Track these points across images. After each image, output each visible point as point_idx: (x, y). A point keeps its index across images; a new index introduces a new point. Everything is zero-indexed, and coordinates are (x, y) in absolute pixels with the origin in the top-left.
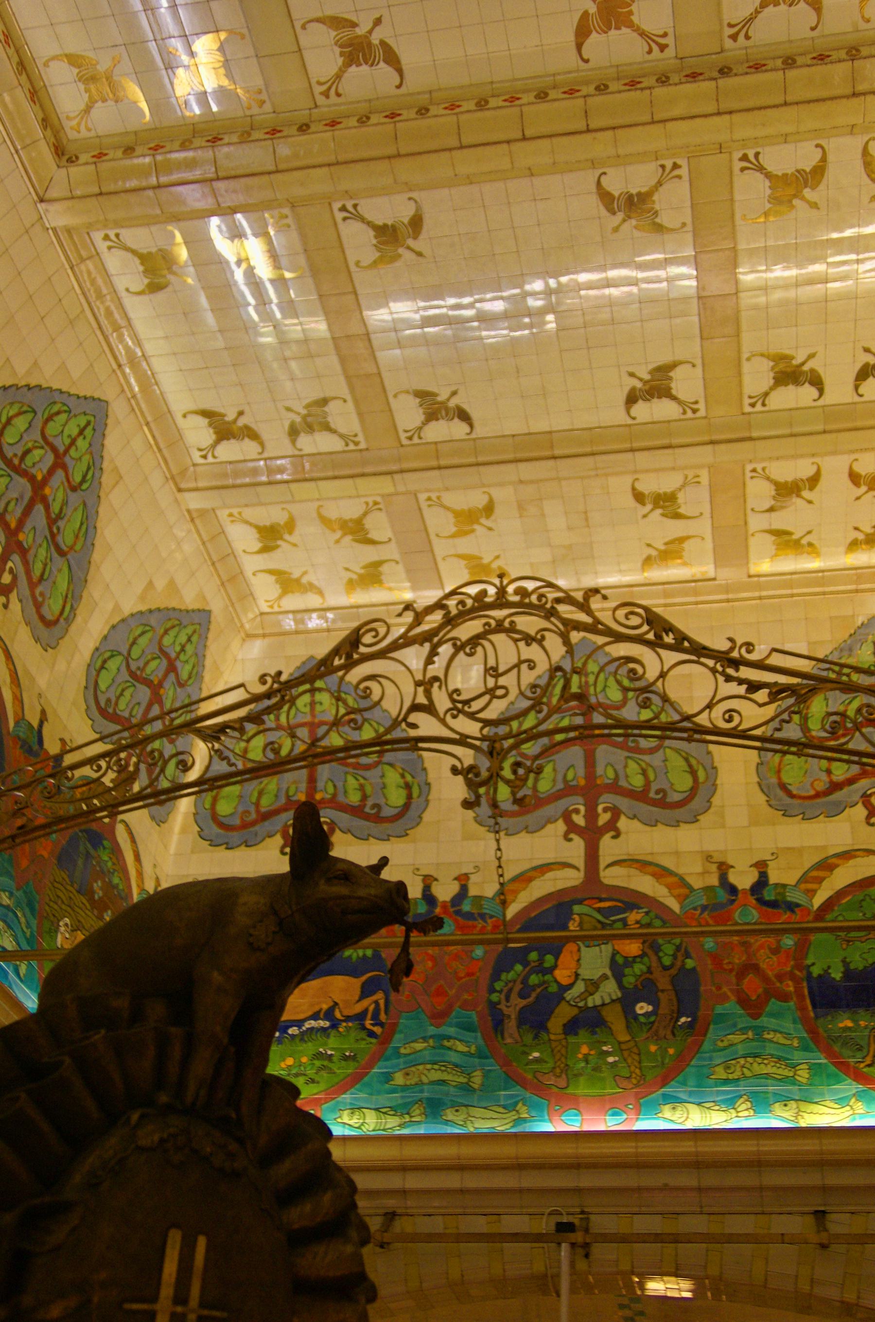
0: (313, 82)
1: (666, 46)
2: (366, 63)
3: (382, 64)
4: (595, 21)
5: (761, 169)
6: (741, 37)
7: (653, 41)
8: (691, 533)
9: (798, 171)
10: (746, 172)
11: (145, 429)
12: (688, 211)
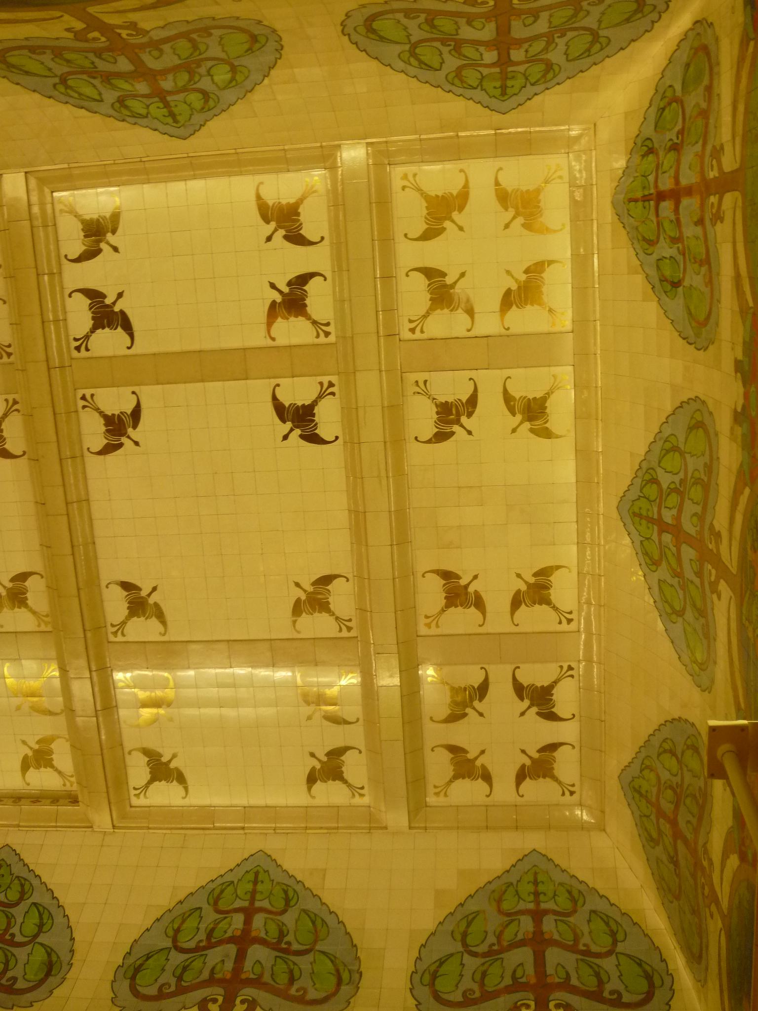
0: (37, 629)
1: (14, 400)
2: (25, 594)
3: (27, 584)
5: (87, 337)
7: (11, 408)
8: (501, 390)
9: (90, 309)
11: (308, 831)
12: (122, 389)
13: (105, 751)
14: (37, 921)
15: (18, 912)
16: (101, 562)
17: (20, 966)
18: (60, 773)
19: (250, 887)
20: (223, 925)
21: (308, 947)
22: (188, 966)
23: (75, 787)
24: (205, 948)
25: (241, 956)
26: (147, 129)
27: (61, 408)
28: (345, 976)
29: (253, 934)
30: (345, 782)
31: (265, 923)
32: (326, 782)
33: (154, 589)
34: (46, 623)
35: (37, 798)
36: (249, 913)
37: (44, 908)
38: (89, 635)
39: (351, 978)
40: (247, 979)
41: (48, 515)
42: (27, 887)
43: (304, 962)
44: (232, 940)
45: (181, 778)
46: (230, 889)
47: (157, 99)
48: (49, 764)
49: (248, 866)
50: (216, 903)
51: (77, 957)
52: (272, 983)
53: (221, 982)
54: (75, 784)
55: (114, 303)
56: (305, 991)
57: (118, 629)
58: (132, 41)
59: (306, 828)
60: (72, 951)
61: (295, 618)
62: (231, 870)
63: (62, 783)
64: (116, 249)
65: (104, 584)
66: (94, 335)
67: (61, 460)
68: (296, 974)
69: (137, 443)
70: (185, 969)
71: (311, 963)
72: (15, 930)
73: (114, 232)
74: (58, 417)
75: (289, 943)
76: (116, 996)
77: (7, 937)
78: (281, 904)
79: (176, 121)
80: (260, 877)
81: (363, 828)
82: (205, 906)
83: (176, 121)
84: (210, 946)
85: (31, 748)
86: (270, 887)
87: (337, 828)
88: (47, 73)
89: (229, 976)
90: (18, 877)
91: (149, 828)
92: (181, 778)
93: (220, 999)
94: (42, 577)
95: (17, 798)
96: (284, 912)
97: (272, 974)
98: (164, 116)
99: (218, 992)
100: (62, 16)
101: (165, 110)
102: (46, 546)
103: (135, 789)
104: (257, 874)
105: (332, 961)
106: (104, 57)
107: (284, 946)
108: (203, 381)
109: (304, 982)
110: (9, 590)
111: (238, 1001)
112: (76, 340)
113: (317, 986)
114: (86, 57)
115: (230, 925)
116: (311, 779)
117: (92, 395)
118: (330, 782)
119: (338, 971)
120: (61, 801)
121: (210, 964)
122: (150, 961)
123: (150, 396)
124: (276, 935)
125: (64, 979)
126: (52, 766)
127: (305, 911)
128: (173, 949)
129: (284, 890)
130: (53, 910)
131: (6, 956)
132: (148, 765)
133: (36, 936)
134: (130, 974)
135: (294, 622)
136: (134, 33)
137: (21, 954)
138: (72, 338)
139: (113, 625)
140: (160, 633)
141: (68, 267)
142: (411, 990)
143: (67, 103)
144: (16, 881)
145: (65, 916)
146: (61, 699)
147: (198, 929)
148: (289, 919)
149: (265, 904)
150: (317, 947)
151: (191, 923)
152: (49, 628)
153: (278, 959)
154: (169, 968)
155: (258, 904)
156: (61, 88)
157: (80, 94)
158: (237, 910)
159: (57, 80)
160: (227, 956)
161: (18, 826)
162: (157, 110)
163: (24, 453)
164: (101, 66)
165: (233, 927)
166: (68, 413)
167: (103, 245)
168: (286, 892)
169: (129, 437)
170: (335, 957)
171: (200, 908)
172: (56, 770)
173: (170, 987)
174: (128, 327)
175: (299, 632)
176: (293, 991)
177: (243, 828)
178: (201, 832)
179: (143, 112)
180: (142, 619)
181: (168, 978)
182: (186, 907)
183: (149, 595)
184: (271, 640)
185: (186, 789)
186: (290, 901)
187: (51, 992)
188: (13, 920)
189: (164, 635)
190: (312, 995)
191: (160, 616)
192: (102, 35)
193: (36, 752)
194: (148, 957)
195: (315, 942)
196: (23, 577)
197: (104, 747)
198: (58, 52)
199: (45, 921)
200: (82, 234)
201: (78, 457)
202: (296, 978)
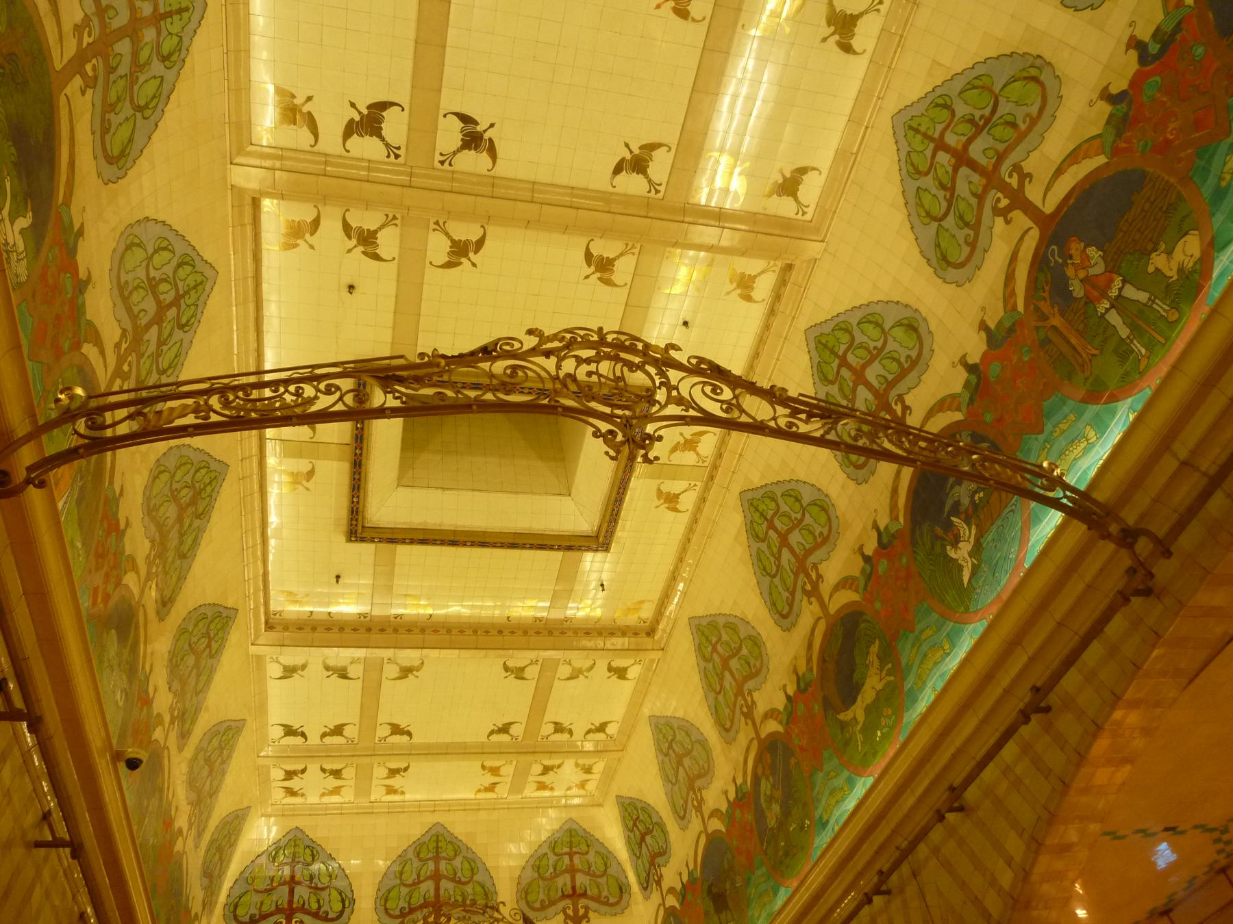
0: (636, 256)
1: (434, 223)
4: (472, 247)
5: (387, 145)
6: (391, 217)
9: (362, 136)
10: (397, 146)
11: (893, 67)
12: (440, 127)
13: (756, 230)
14: (871, 326)
15: (859, 338)
16: (592, 186)
17: (900, 350)
18: (762, 272)
19: (919, 137)
20: (940, 172)
21: (992, 102)
22: (960, 214)
23: (779, 263)
24: (952, 195)
25: (973, 165)
26: (194, 39)
27: (446, 185)
28: (1033, 72)
29: (959, 147)
30: (861, 15)
31: (955, 133)
32: (854, 35)
33: (627, 145)
34: (633, 247)
35: (777, 297)
36: (941, 145)
37: (864, 317)
38: (651, 214)
39: (1037, 67)
40: (994, 165)
41: (539, 221)
42: (843, 326)
43: (1004, 108)
44: (956, 169)
45: (803, 171)
46: (914, 156)
47: (162, 23)
48: (753, 279)
49: (901, 133)
50: (918, 172)
51: (912, 303)
52: (1007, 144)
53: (986, 190)
54: (777, 262)
55: (360, 113)
56: (1028, 115)
57: (655, 188)
58: (97, 33)
59: (890, 67)
60: (906, 306)
61: (690, 19)
62: (898, 150)
63: (771, 273)
64: (309, 99)
65: (611, 189)
66: (386, 139)
67: (492, 197)
68: (1009, 118)
69: (492, 125)
70: (961, 218)
71: (1008, 101)
72: (872, 345)
73: (293, 96)
74: (454, 189)
75: (982, 117)
76: (957, 282)
77: (875, 352)
78: (945, 114)
79: (187, 9)
80: (915, 126)
81: (912, 9)
82: (918, 183)
83: (187, 9)
84: (952, 190)
85: (735, 289)
86: (927, 119)
87: (901, 36)
88: (132, 121)
89: (984, 181)
90: (833, 330)
91: (835, 212)
92: (803, 171)
93: (999, 195)
94: (592, 240)
95: (772, 312)
96: (953, 113)
97: (1000, 142)
98: (181, 20)
99: (994, 194)
100: (66, 95)
101: (174, 17)
102: (566, 229)
103: (797, 214)
104: (911, 128)
105: (1015, 81)
106: (114, 65)
107: (981, 123)
108: (444, 47)
109: (1020, 113)
110: (597, 270)
111: (1007, 180)
112: (388, 156)
113: (1029, 102)
114: (114, 82)
115: (943, 166)
116: (847, 48)
117: (441, 154)
118: (856, 30)
119: (1025, 78)
120: (787, 278)
121: (967, 195)
122: (942, 246)
123: (451, 101)
124: (969, 126)
125: (925, 319)
126: (755, 277)
127: (961, 93)
128: (941, 223)
129: (934, 107)
130: (869, 310)
131: (888, 358)
132: (780, 196)
133: (883, 330)
134: (944, 265)
135: (694, 20)
136: (87, 29)
137: (891, 345)
138: (386, 160)
139: (649, 192)
140: (668, 151)
141: (320, 147)
142: (1076, 10)
143: (163, 111)
144: (836, 332)
145: (877, 303)
146: (702, 254)
147: (934, 195)
148: (961, 110)
149: (940, 128)
150: (997, 92)
151: (927, 199)
152: (638, 246)
153: (991, 132)
154: (955, 231)
155: (936, 135)
156: (148, 113)
157: (154, 97)
158: (934, 156)
159: (139, 115)
160: (967, 177)
161: (794, 318)
162: (174, 25)
163: (482, 226)
164: (124, 69)
165: (946, 164)
166: (453, 180)
167: (305, 109)
168: (937, 105)
169: (485, 131)
170: (1013, 77)
171: (919, 188)
172: (760, 274)
173: (969, 235)
174: (384, 106)
175: (704, 19)
176: (1023, 127)
177: (867, 127)
178: (855, 166)
179: (175, 39)
180: (650, 164)
181: (961, 234)
182: (912, 200)
183: (631, 152)
184: (703, 49)
185: (814, 169)
186: (946, 104)
187: (930, 332)
188: (864, 344)
189: (670, 148)
190: (1034, 110)
191: (652, 147)
192: (90, 62)
193: (739, 286)
194: (938, 246)
195: (992, 92)
196: (588, 256)
197: (752, 229)
198: (109, 107)
199: (874, 320)
200: (292, 126)
201: (494, 181)
202: (1013, 120)
